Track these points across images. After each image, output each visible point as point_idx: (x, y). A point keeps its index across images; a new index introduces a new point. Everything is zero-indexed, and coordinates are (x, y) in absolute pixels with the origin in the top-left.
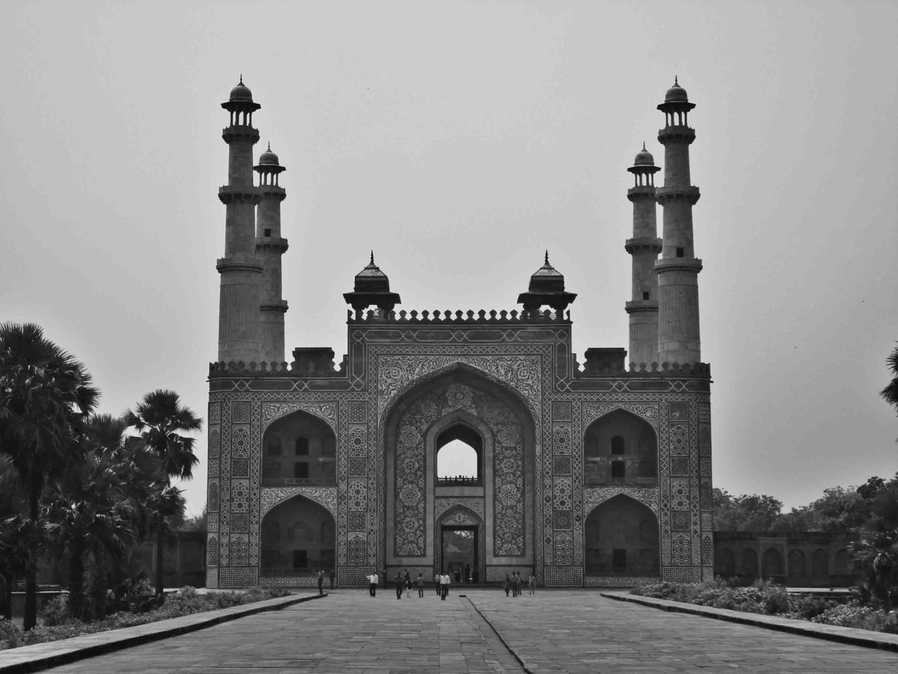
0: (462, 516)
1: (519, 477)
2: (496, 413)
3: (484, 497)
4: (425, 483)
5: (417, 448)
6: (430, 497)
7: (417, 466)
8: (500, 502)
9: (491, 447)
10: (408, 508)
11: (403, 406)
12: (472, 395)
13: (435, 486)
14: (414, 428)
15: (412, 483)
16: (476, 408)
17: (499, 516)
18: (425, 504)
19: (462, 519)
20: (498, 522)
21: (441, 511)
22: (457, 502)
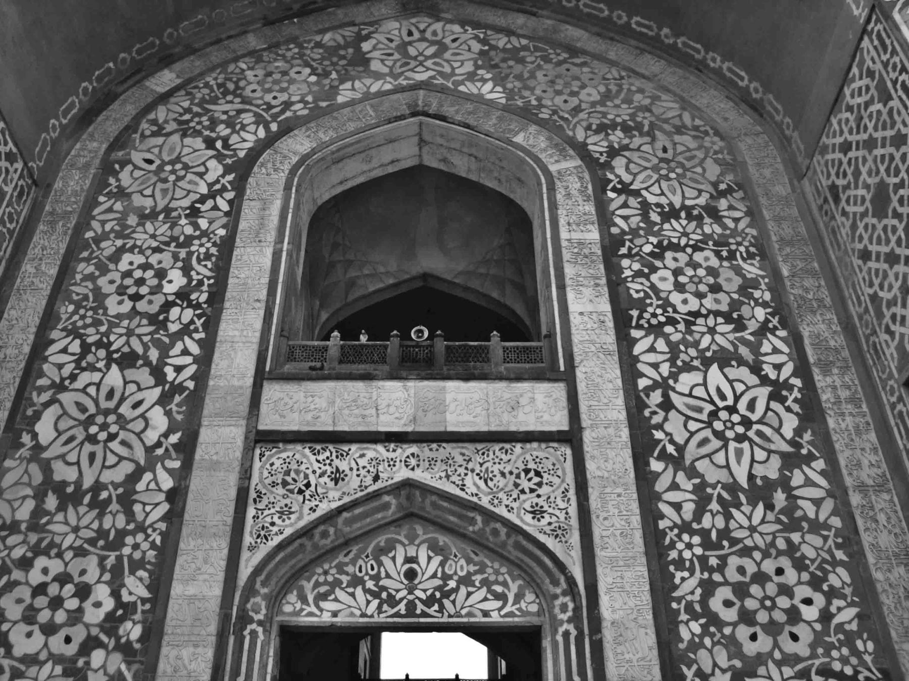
0: (429, 565)
1: (764, 330)
2: (591, 94)
3: (571, 437)
4: (205, 361)
5: (194, 213)
6: (221, 438)
7: (176, 280)
8: (676, 462)
9: (590, 208)
10: (70, 497)
11: (165, 79)
12: (476, 47)
13: (260, 377)
14: (199, 143)
15: (128, 360)
16: (499, 80)
17: (687, 548)
18: (183, 475)
19: (426, 586)
20: (688, 586)
21: (281, 520)
22: (399, 466)
